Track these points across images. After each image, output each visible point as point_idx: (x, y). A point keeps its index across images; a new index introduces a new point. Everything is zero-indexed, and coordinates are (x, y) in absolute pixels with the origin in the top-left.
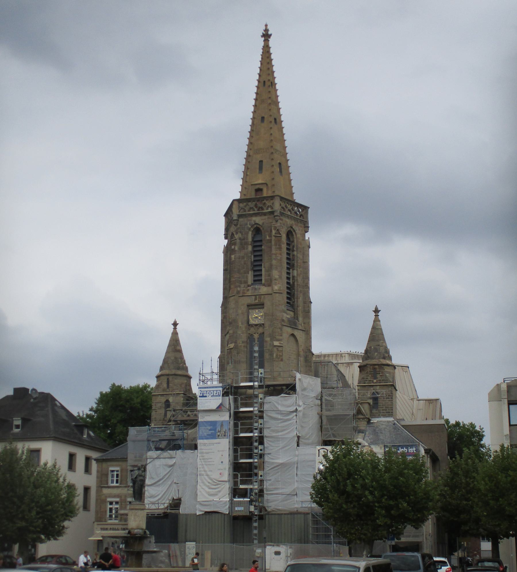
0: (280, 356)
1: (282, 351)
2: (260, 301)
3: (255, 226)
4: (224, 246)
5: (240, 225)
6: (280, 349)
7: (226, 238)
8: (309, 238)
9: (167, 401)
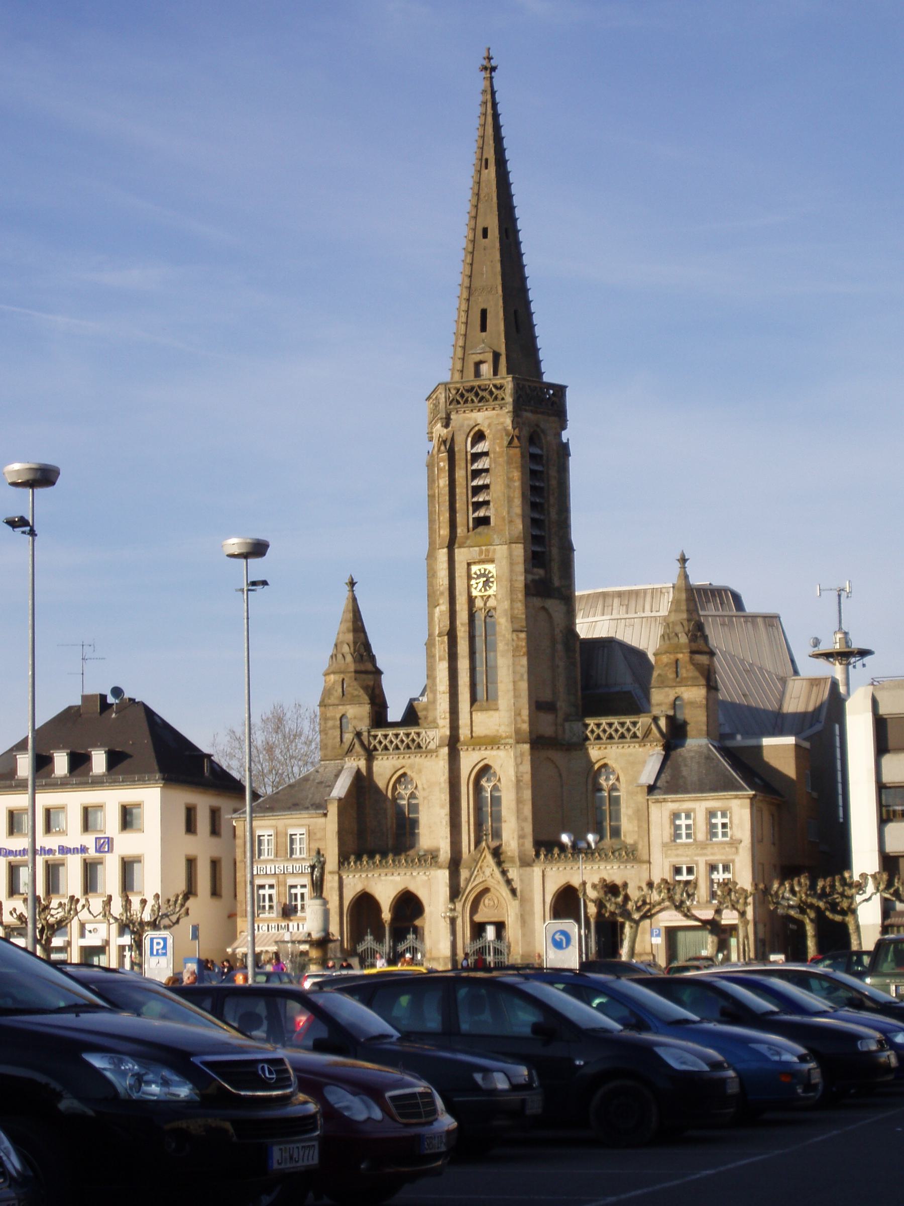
2: (488, 556)
4: (429, 452)
8: (568, 440)
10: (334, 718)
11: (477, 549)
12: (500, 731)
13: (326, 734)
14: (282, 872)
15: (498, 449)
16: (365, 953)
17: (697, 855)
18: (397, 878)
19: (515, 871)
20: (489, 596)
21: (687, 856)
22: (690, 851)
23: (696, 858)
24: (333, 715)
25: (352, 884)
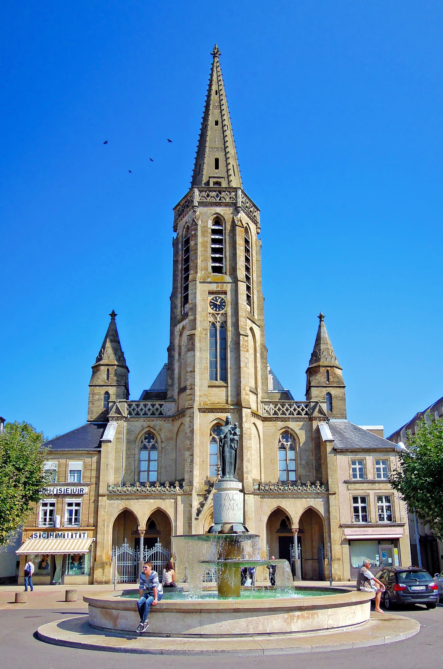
0: (246, 346)
1: (248, 341)
2: (223, 289)
4: (173, 238)
5: (200, 213)
6: (246, 338)
9: (107, 393)
10: (99, 394)
11: (216, 284)
13: (93, 404)
14: (63, 493)
16: (122, 557)
22: (365, 486)
24: (98, 391)
25: (116, 504)
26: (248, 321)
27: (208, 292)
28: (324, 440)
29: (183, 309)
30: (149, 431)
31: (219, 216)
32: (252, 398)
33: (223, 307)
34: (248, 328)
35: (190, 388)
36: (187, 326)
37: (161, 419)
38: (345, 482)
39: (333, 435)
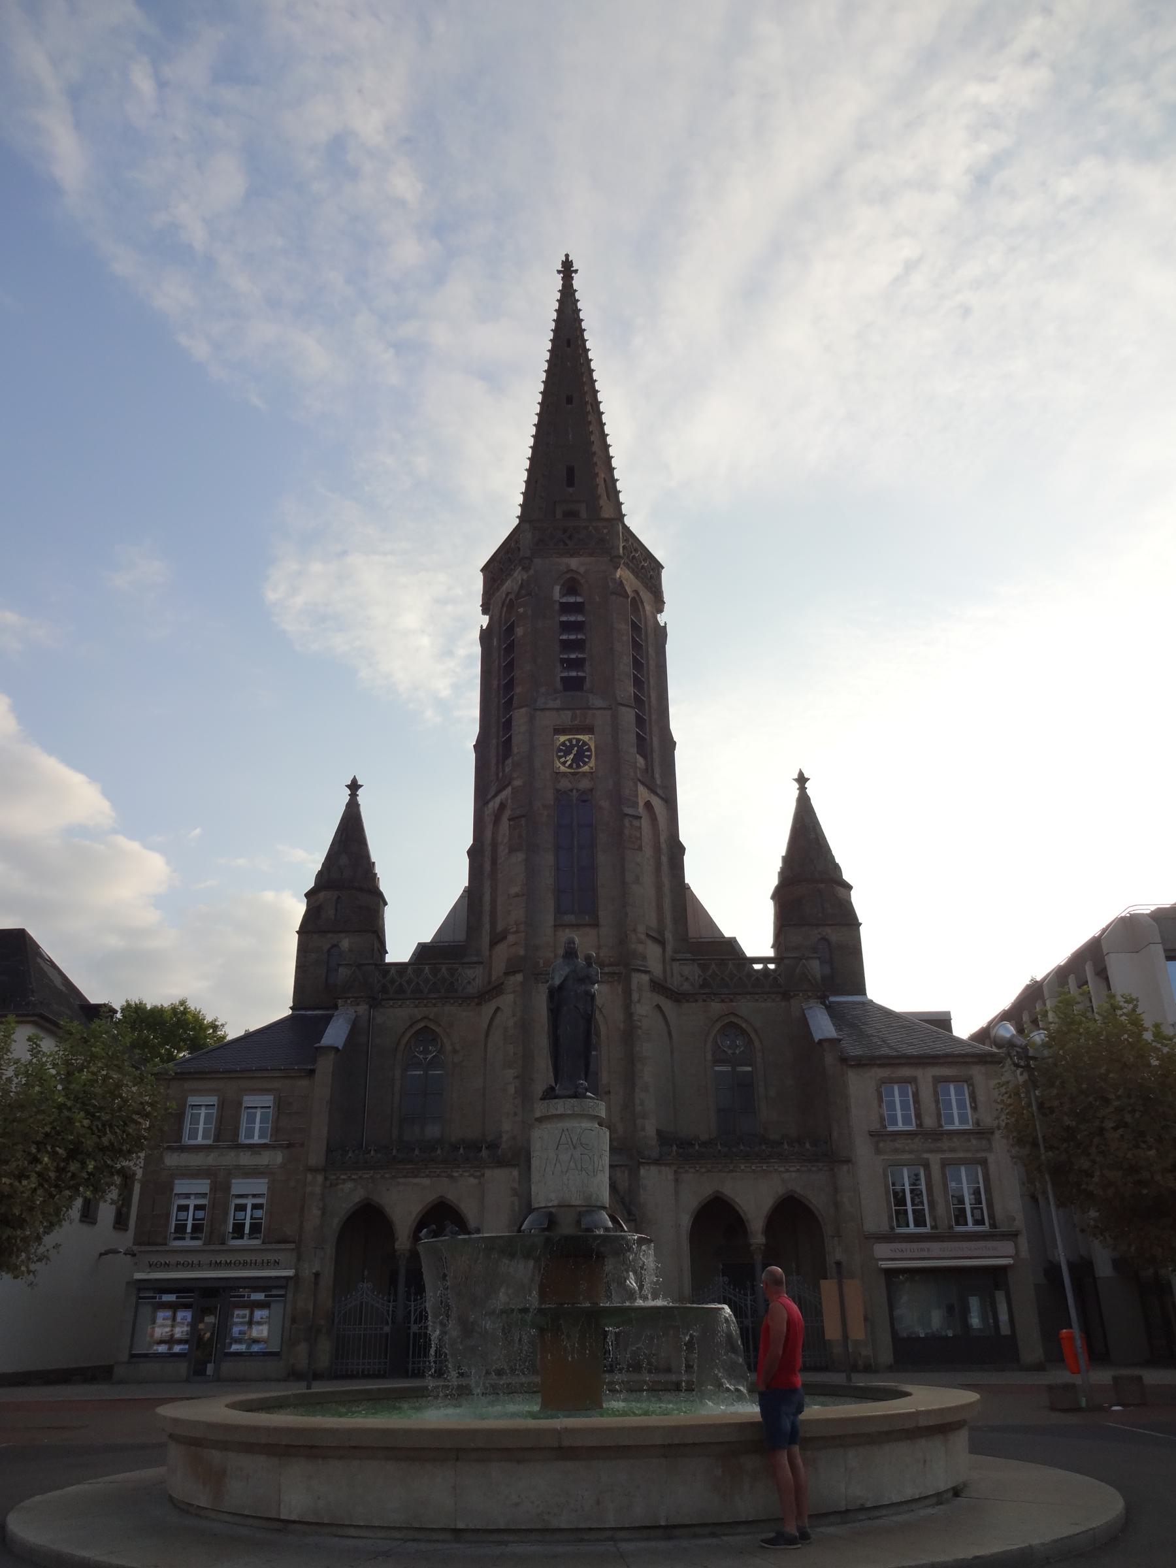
1: (640, 828)
3: (568, 576)
4: (482, 627)
6: (636, 823)
7: (486, 609)
8: (666, 624)
11: (569, 713)
12: (602, 955)
15: (598, 599)
17: (931, 1151)
18: (426, 1182)
19: (626, 1172)
20: (584, 774)
21: (911, 1152)
23: (926, 1156)
26: (641, 788)
27: (555, 729)
28: (816, 1040)
29: (500, 767)
30: (426, 1026)
31: (575, 576)
32: (653, 952)
33: (587, 760)
34: (641, 804)
35: (515, 929)
36: (509, 801)
37: (452, 1001)
38: (872, 1134)
39: (838, 1027)
